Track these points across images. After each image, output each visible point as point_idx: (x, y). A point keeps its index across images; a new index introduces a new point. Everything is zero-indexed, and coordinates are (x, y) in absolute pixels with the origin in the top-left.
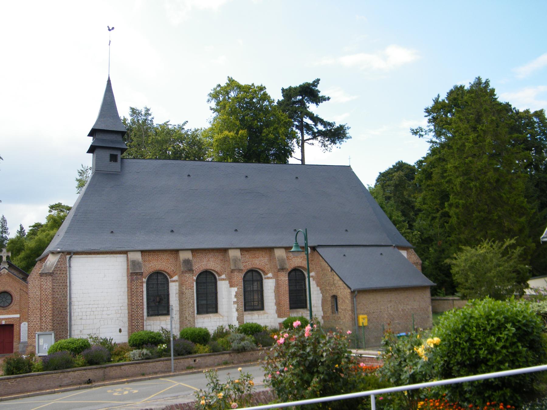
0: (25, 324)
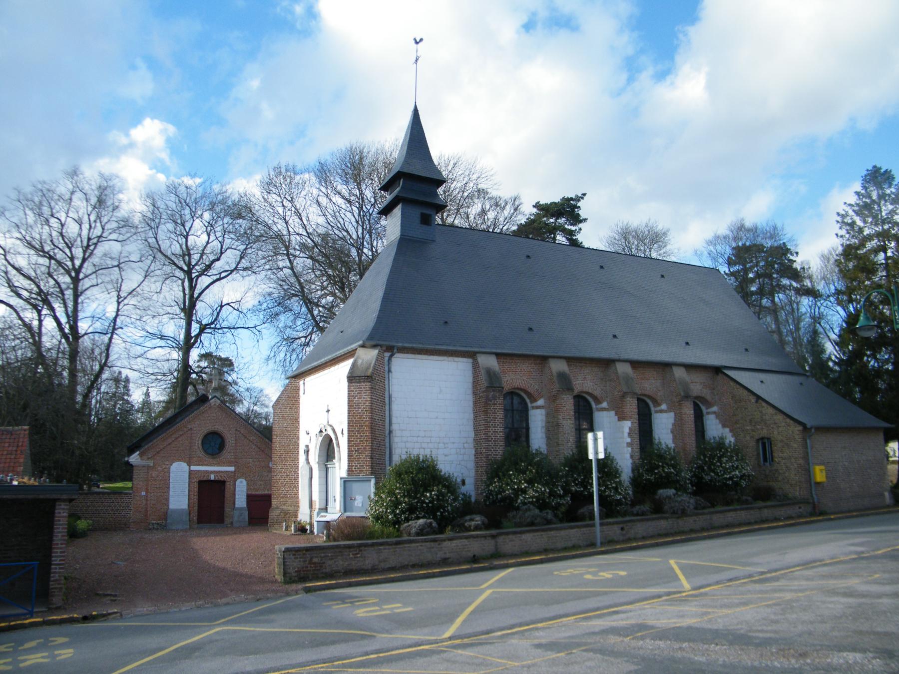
0: (241, 482)
